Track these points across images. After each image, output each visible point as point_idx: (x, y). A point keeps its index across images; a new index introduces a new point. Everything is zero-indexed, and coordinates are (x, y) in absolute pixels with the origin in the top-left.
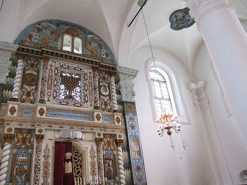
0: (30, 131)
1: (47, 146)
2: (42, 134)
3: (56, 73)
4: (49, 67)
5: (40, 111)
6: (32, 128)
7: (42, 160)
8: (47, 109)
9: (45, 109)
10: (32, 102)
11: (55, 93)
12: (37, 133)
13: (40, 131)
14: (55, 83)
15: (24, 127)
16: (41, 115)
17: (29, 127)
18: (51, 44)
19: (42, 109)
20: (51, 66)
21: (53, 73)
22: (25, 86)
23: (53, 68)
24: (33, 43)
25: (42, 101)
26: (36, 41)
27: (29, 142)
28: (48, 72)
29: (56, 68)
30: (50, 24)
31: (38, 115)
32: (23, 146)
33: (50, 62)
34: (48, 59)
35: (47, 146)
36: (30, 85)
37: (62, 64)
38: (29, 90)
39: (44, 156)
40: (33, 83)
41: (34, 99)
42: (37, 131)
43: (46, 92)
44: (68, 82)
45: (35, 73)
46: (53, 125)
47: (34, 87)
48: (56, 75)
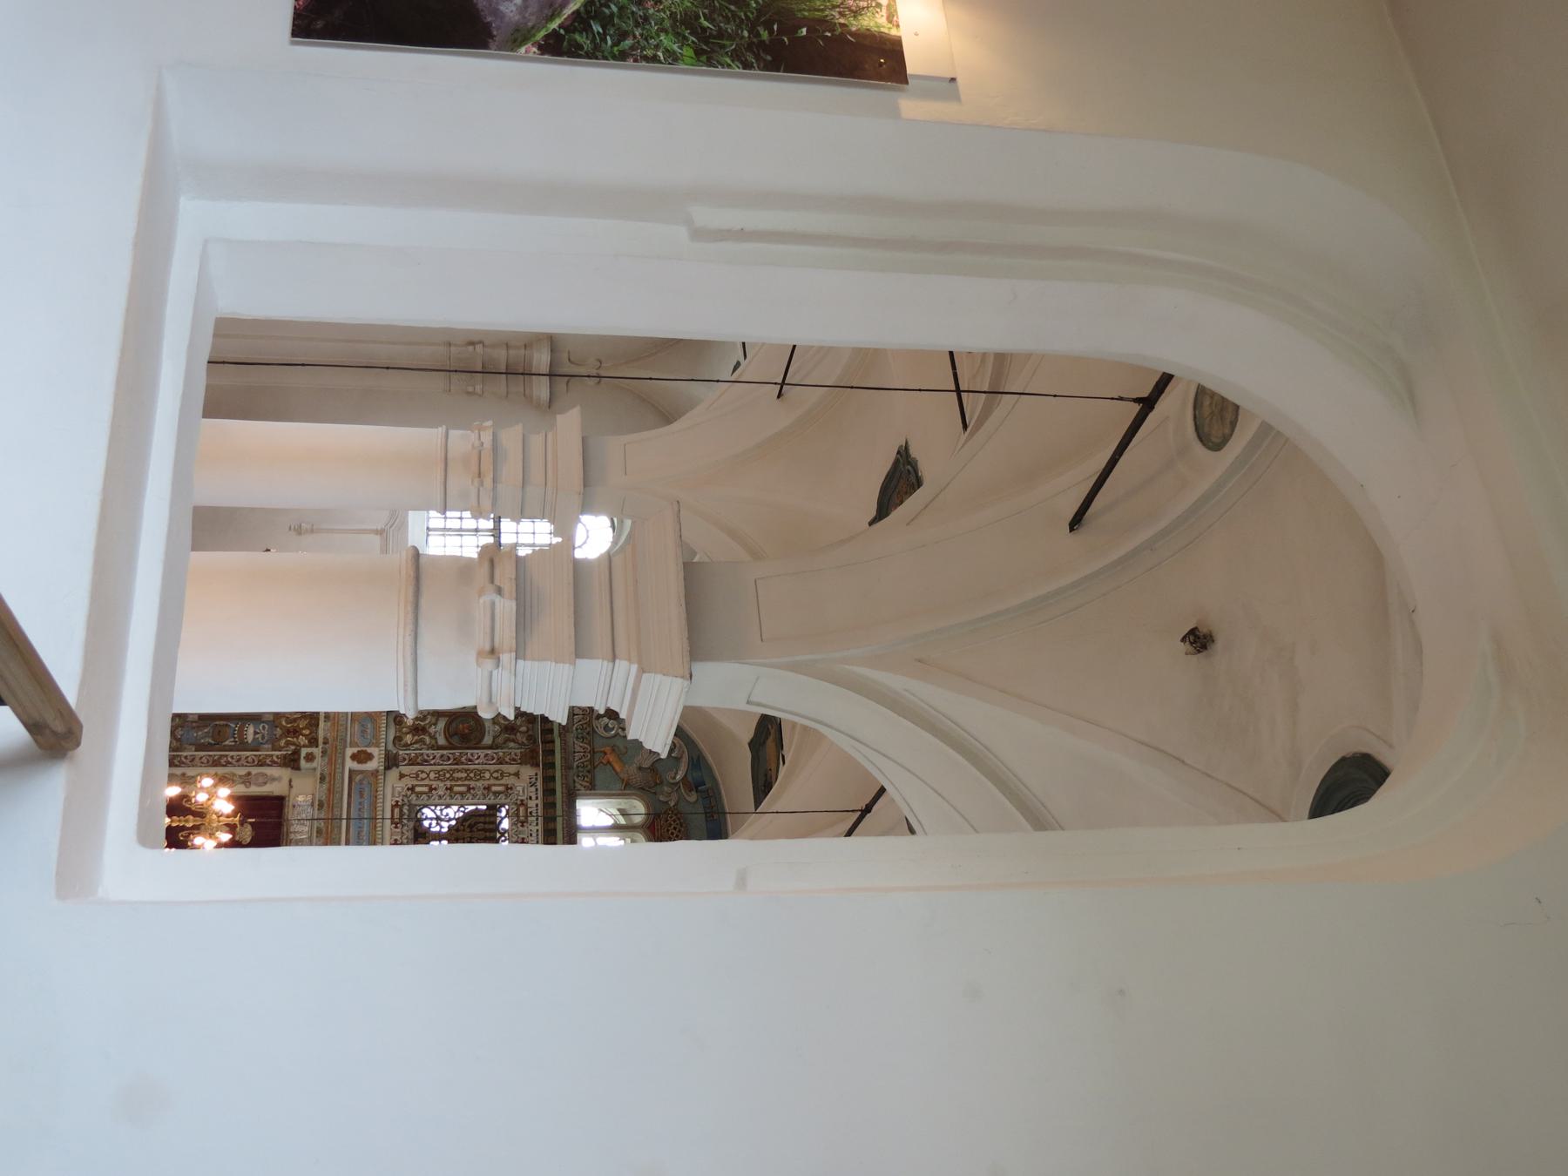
0: (313, 742)
1: (274, 779)
2: (303, 763)
3: (494, 789)
4: (512, 769)
5: (365, 752)
6: (321, 740)
7: (242, 771)
8: (375, 773)
9: (372, 765)
10: (398, 739)
11: (425, 789)
12: (304, 752)
13: (310, 758)
14: (456, 789)
15: (322, 724)
16: (354, 757)
17: (321, 734)
18: (600, 775)
19: (369, 757)
20: (517, 775)
21: (492, 781)
22: (441, 724)
23: (510, 781)
24: (589, 724)
25: (391, 762)
26: (601, 731)
27: (288, 744)
28: (493, 768)
29: (508, 788)
30: (685, 759)
31: (350, 751)
32: (279, 731)
33: (527, 772)
34: (530, 758)
35: (274, 779)
36: (448, 733)
37: (532, 804)
38: (432, 730)
39: (249, 774)
40: (455, 741)
41: (406, 745)
42: (309, 750)
43: (427, 769)
44: (470, 826)
45: (488, 740)
46: (325, 786)
47: (442, 741)
48: (488, 788)
